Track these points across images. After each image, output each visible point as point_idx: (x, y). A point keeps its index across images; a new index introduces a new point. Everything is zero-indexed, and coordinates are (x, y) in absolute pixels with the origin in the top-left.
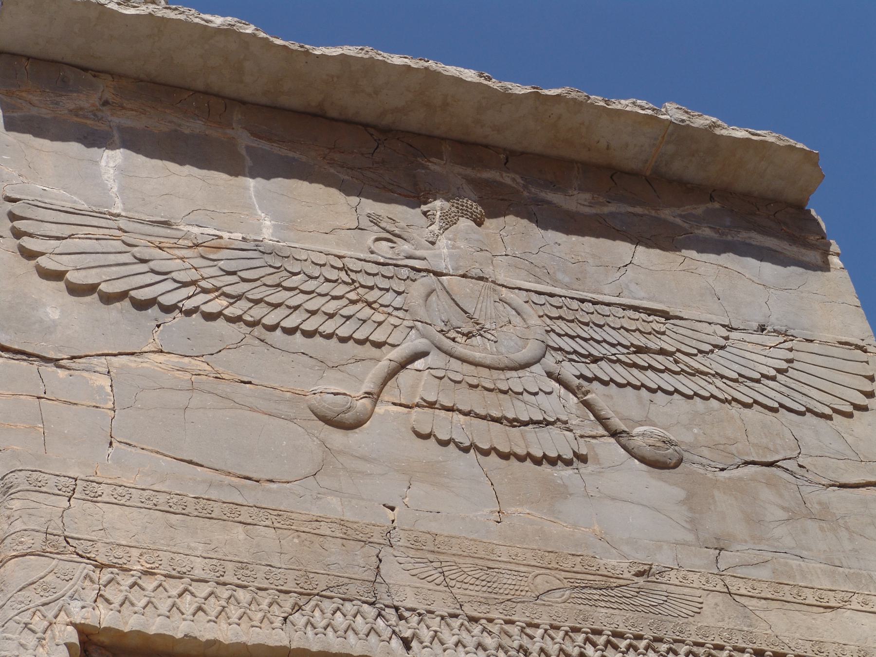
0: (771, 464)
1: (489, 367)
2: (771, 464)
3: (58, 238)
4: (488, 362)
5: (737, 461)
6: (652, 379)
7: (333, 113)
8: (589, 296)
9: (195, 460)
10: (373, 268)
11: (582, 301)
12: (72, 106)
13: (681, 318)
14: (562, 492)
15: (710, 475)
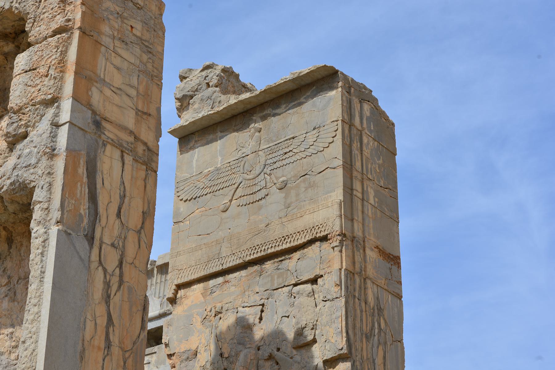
0: (306, 174)
1: (253, 179)
2: (306, 174)
3: (183, 190)
4: (252, 178)
5: (299, 177)
6: (287, 161)
7: (236, 114)
8: (277, 142)
9: (200, 234)
10: (237, 161)
11: (276, 145)
12: (189, 147)
13: (296, 137)
14: (260, 208)
15: (292, 186)
